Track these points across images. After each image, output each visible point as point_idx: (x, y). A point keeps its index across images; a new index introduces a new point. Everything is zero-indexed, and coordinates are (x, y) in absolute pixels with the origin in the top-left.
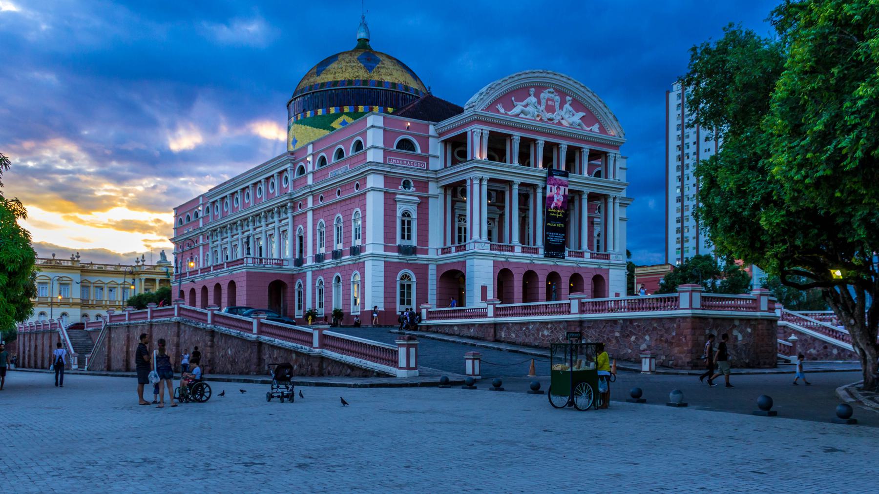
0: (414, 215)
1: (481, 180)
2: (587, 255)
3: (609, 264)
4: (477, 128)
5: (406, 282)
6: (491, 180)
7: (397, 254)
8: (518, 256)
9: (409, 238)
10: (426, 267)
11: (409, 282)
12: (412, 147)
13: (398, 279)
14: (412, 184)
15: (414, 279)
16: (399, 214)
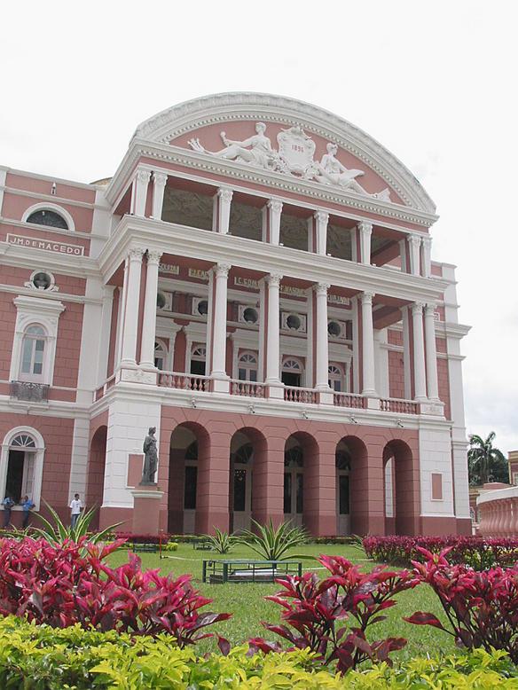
0: (52, 331)
1: (145, 257)
2: (373, 404)
3: (418, 422)
4: (144, 171)
5: (23, 447)
6: (166, 259)
7: (7, 398)
8: (220, 399)
9: (38, 369)
10: (69, 424)
11: (30, 449)
12: (65, 226)
13: (7, 442)
14: (53, 280)
15: (40, 444)
16: (20, 327)
